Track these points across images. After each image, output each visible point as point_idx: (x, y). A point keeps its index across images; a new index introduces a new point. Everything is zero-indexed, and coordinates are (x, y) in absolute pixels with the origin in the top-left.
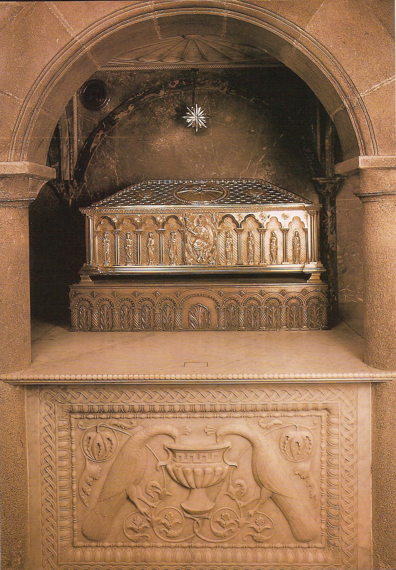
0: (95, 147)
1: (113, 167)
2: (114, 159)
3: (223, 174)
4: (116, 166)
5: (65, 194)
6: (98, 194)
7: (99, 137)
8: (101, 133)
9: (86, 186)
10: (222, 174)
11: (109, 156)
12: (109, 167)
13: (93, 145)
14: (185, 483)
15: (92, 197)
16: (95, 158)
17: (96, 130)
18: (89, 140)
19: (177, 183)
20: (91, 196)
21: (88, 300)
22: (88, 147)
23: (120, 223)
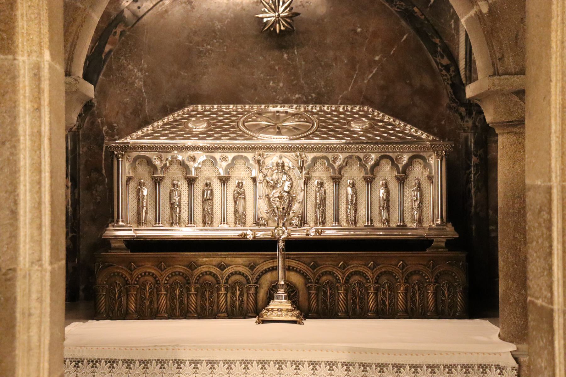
0: (110, 51)
1: (139, 83)
2: (141, 70)
3: (312, 96)
4: (145, 82)
6: (115, 125)
7: (117, 37)
8: (119, 30)
9: (96, 112)
10: (310, 98)
11: (132, 66)
12: (133, 83)
13: (108, 48)
15: (106, 130)
16: (110, 69)
19: (241, 109)
20: (104, 128)
21: (122, 276)
23: (165, 168)
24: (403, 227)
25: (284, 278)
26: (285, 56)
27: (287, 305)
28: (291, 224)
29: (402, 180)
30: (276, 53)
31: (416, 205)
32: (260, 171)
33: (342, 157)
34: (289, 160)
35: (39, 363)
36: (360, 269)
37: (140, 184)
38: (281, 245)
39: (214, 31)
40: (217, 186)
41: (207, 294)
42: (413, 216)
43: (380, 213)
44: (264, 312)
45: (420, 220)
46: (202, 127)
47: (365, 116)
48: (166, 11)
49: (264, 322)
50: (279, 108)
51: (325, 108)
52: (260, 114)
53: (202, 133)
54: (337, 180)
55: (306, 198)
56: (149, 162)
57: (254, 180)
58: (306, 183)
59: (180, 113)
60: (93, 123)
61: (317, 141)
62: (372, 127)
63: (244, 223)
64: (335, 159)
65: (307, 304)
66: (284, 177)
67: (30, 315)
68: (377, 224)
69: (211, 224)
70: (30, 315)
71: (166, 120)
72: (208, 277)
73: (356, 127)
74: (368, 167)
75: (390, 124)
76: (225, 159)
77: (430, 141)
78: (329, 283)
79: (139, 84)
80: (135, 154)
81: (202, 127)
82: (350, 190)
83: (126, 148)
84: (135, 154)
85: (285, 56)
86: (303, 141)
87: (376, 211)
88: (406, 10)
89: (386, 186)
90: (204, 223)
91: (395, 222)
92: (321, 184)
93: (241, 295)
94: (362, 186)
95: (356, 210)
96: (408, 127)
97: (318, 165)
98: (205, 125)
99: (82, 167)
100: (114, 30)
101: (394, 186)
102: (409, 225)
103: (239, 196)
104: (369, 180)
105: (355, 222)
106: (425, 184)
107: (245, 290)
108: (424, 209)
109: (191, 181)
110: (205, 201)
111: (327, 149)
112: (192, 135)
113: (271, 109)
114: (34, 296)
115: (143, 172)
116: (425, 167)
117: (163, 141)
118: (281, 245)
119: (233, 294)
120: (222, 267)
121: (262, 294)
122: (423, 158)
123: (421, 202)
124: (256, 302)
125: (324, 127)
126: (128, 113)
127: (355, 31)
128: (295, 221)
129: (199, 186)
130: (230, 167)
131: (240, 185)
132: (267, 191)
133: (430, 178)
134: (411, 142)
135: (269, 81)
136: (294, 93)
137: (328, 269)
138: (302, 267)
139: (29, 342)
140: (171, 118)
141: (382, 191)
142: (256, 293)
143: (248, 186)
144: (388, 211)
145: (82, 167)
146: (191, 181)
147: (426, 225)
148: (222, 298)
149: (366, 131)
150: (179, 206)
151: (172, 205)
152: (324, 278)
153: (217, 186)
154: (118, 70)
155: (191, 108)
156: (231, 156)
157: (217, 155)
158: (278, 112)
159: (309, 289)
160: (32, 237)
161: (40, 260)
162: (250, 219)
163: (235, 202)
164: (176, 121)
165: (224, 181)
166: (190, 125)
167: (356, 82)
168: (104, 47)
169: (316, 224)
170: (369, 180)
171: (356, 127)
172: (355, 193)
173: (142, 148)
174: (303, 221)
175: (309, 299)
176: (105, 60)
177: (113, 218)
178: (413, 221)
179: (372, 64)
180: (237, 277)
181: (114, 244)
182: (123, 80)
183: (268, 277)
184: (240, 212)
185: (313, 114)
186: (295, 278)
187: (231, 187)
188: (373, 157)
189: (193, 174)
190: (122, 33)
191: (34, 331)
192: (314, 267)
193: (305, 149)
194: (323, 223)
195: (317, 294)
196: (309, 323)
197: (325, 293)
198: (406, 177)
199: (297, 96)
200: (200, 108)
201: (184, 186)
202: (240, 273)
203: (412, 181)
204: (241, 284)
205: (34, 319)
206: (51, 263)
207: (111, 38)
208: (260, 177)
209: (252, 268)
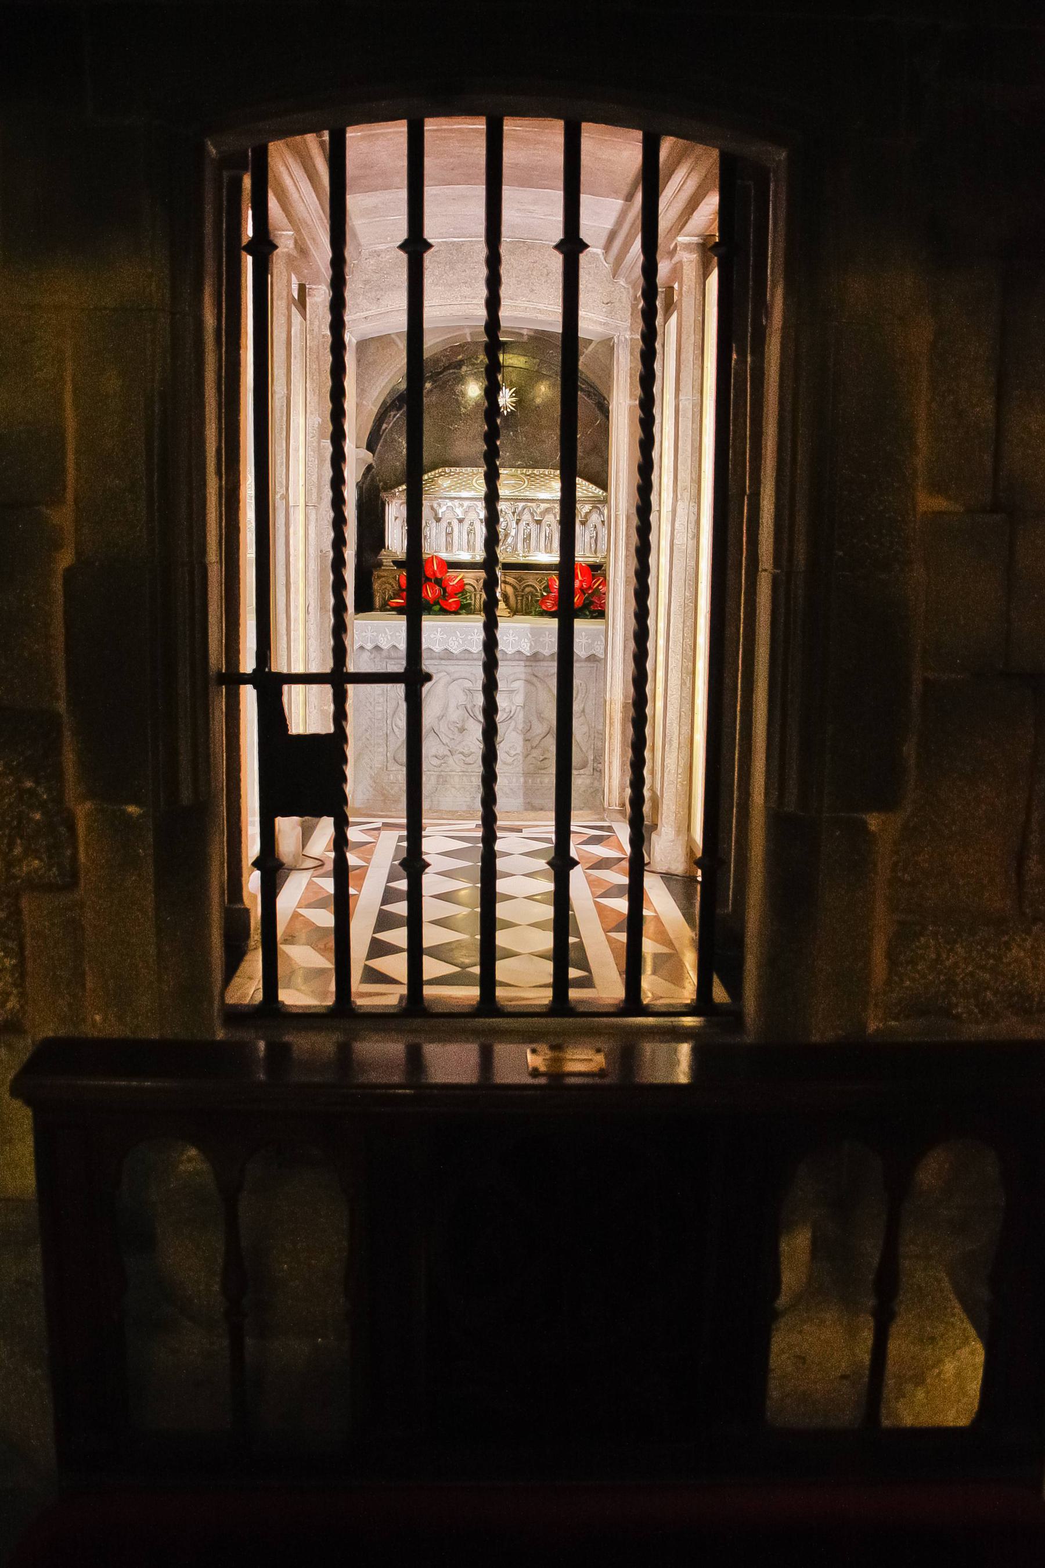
13: (384, 426)
31: (593, 541)
40: (455, 523)
51: (535, 472)
58: (517, 523)
59: (433, 473)
63: (474, 550)
65: (515, 606)
69: (451, 551)
76: (462, 505)
77: (603, 496)
78: (530, 592)
90: (447, 549)
96: (591, 486)
98: (449, 482)
100: (389, 414)
106: (599, 526)
107: (473, 596)
110: (447, 534)
116: (600, 515)
122: (598, 508)
129: (444, 524)
130: (466, 512)
131: (472, 524)
133: (603, 522)
137: (530, 583)
146: (438, 520)
153: (455, 524)
155: (440, 470)
156: (466, 503)
157: (456, 502)
159: (516, 596)
163: (468, 535)
165: (461, 521)
168: (381, 426)
169: (524, 552)
175: (517, 603)
182: (394, 449)
184: (471, 543)
186: (510, 590)
187: (466, 525)
189: (440, 516)
193: (517, 500)
195: (522, 600)
197: (527, 599)
199: (519, 463)
202: (472, 585)
203: (590, 524)
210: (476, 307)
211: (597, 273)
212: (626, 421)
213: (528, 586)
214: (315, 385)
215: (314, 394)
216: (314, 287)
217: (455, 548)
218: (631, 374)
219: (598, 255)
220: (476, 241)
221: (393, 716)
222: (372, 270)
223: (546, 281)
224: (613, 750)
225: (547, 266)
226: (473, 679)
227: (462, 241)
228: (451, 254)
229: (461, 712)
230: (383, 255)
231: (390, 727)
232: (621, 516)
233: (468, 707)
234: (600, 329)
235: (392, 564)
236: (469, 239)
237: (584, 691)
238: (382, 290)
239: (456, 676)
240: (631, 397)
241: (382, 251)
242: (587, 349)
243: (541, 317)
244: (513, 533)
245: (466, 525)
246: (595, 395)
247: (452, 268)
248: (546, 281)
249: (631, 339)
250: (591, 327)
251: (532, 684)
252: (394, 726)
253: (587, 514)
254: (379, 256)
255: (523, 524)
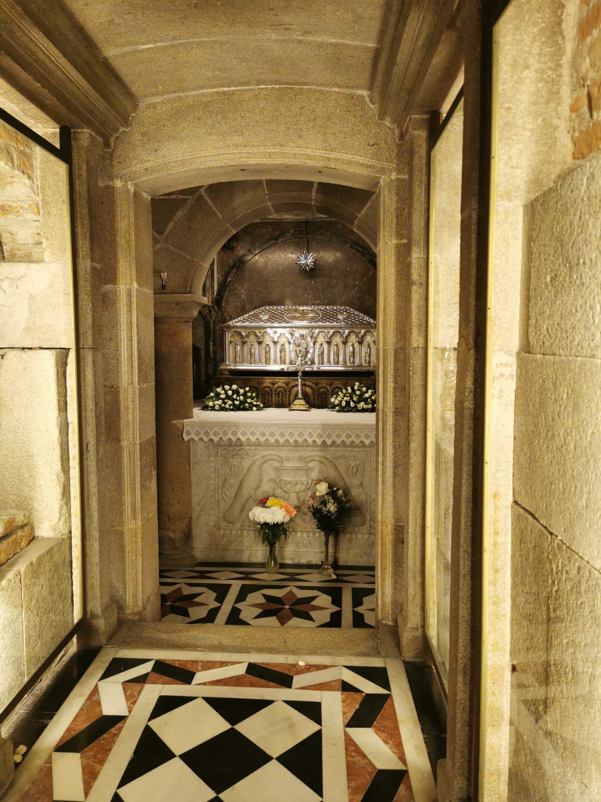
0: (230, 281)
5: (208, 316)
8: (234, 271)
13: (229, 279)
14: (286, 489)
16: (230, 289)
17: (232, 268)
18: (226, 275)
22: (225, 280)
23: (247, 336)
24: (361, 365)
25: (302, 390)
26: (313, 282)
27: (303, 402)
28: (307, 364)
29: (360, 343)
30: (308, 281)
32: (292, 338)
33: (332, 331)
34: (304, 332)
35: (134, 431)
36: (339, 386)
37: (236, 344)
38: (300, 374)
39: (279, 271)
40: (271, 345)
41: (267, 396)
42: (366, 360)
43: (350, 359)
44: (292, 405)
45: (369, 363)
46: (266, 317)
47: (346, 312)
48: (256, 262)
49: (292, 410)
50: (305, 308)
52: (296, 311)
53: (266, 320)
54: (329, 343)
55: (314, 351)
56: (240, 334)
57: (289, 343)
58: (314, 344)
59: (258, 310)
60: (222, 315)
61: (320, 324)
62: (348, 317)
63: (285, 363)
64: (328, 333)
66: (303, 341)
67: (128, 408)
68: (348, 364)
70: (128, 408)
71: (250, 313)
72: (267, 389)
73: (340, 317)
74: (344, 336)
75: (357, 315)
78: (324, 392)
79: (243, 296)
80: (234, 330)
81: (266, 317)
82: (335, 347)
83: (229, 327)
84: (234, 330)
85: (313, 282)
86: (313, 324)
87: (348, 358)
88: (371, 260)
89: (353, 345)
90: (266, 363)
91: (357, 362)
92: (322, 345)
93: (282, 397)
94: (341, 346)
95: (338, 358)
97: (320, 336)
99: (218, 336)
101: (357, 346)
102: (364, 364)
103: (282, 350)
104: (345, 343)
105: (338, 363)
106: (372, 345)
108: (372, 357)
109: (260, 343)
110: (266, 352)
111: (324, 328)
112: (261, 320)
113: (301, 308)
114: (130, 400)
115: (237, 339)
117: (247, 324)
118: (300, 374)
119: (279, 397)
120: (273, 384)
121: (292, 398)
122: (371, 332)
123: (370, 353)
124: (289, 401)
125: (324, 317)
126: (238, 310)
127: (346, 270)
128: (309, 363)
129: (264, 345)
131: (283, 345)
132: (295, 348)
134: (366, 324)
135: (304, 294)
136: (316, 300)
137: (324, 385)
138: (311, 384)
139: (128, 421)
140: (253, 313)
141: (351, 349)
142: (289, 397)
143: (287, 345)
144: (354, 357)
145: (218, 336)
147: (371, 365)
148: (274, 399)
149: (344, 319)
150: (254, 355)
151: (251, 354)
152: (322, 390)
154: (234, 290)
158: (304, 310)
159: (314, 395)
160: (128, 371)
161: (132, 383)
162: (288, 361)
164: (255, 314)
165: (275, 343)
166: (261, 316)
167: (347, 294)
170: (345, 343)
171: (340, 317)
172: (338, 349)
173: (237, 327)
174: (313, 362)
176: (228, 285)
177: (223, 360)
178: (366, 363)
179: (355, 286)
180: (280, 389)
181: (224, 373)
183: (295, 389)
185: (321, 310)
186: (308, 390)
187: (279, 346)
188: (347, 331)
190: (236, 272)
191: (130, 416)
192: (317, 384)
193: (313, 328)
194: (322, 364)
195: (318, 397)
196: (314, 411)
197: (322, 397)
198: (363, 341)
200: (267, 308)
201: (256, 346)
202: (281, 387)
203: (365, 343)
204: (282, 392)
205: (130, 411)
206: (139, 384)
207: (230, 275)
208: (292, 342)
209: (287, 384)
210: (248, 155)
211: (363, 116)
212: (393, 260)
213: (323, 387)
214: (86, 230)
215: (85, 240)
216: (79, 130)
217: (272, 362)
218: (397, 214)
219: (364, 97)
220: (246, 90)
221: (223, 487)
222: (150, 123)
223: (314, 127)
224: (385, 568)
225: (314, 111)
226: (280, 460)
227: (233, 91)
228: (223, 104)
229: (271, 484)
230: (159, 107)
231: (220, 495)
232: (389, 350)
233: (277, 480)
234: (365, 172)
235: (228, 373)
236: (240, 88)
237: (362, 470)
238: (159, 141)
239: (268, 458)
240: (397, 237)
241: (158, 103)
242: (359, 213)
243: (310, 163)
244: (311, 351)
245: (279, 346)
246: (368, 254)
247: (224, 118)
248: (314, 127)
249: (397, 179)
250: (357, 171)
251: (324, 464)
252: (223, 495)
253: (363, 337)
254: (155, 108)
255: (318, 346)
